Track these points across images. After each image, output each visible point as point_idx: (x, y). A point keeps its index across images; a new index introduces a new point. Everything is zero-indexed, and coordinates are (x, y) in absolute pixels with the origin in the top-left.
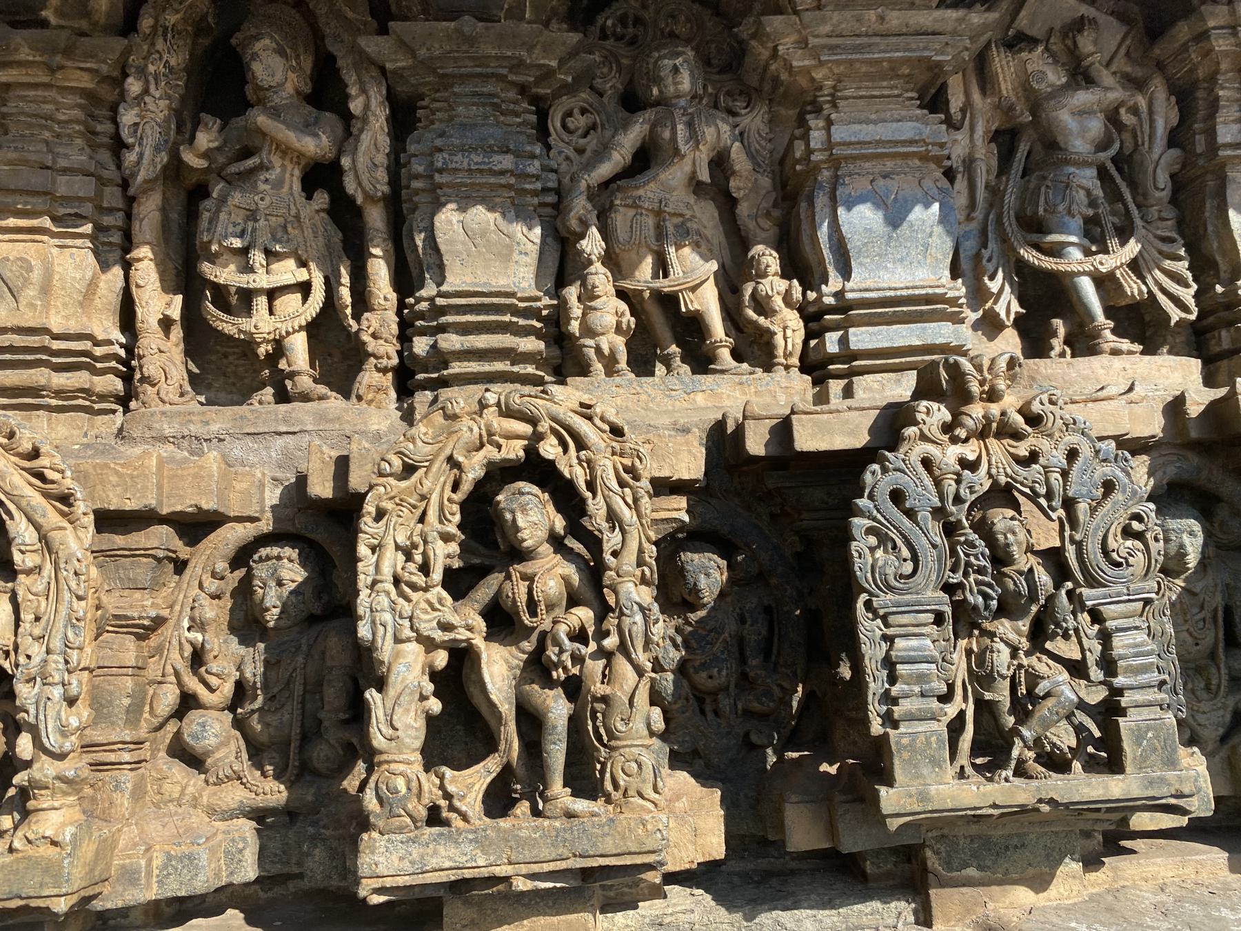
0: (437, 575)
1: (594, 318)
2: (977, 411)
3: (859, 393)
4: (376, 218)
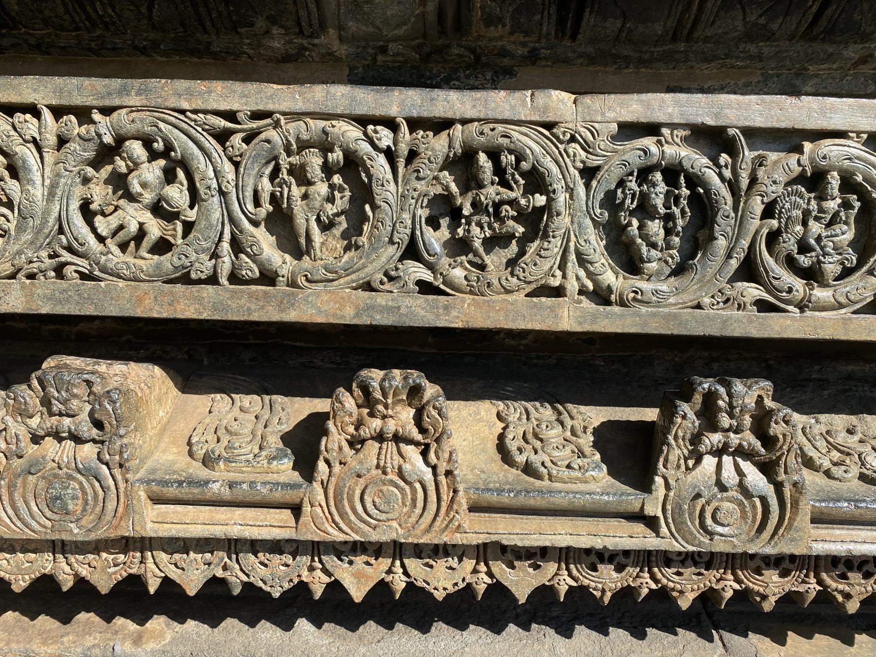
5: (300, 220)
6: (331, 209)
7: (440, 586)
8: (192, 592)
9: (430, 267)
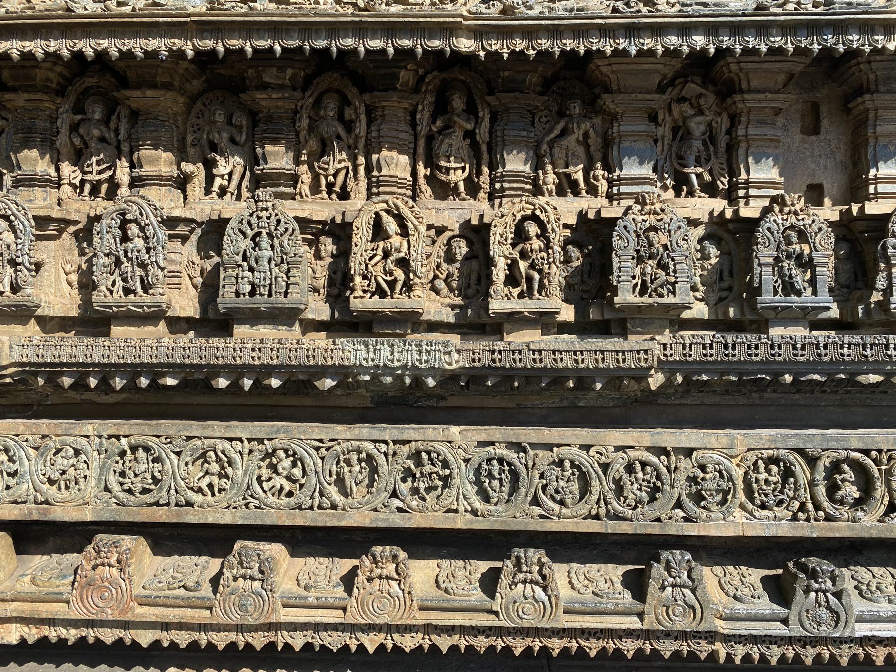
0: (509, 241)
1: (547, 179)
2: (648, 207)
3: (622, 204)
4: (484, 148)
5: (348, 482)
6: (360, 477)
7: (407, 645)
8: (297, 649)
9: (402, 501)
